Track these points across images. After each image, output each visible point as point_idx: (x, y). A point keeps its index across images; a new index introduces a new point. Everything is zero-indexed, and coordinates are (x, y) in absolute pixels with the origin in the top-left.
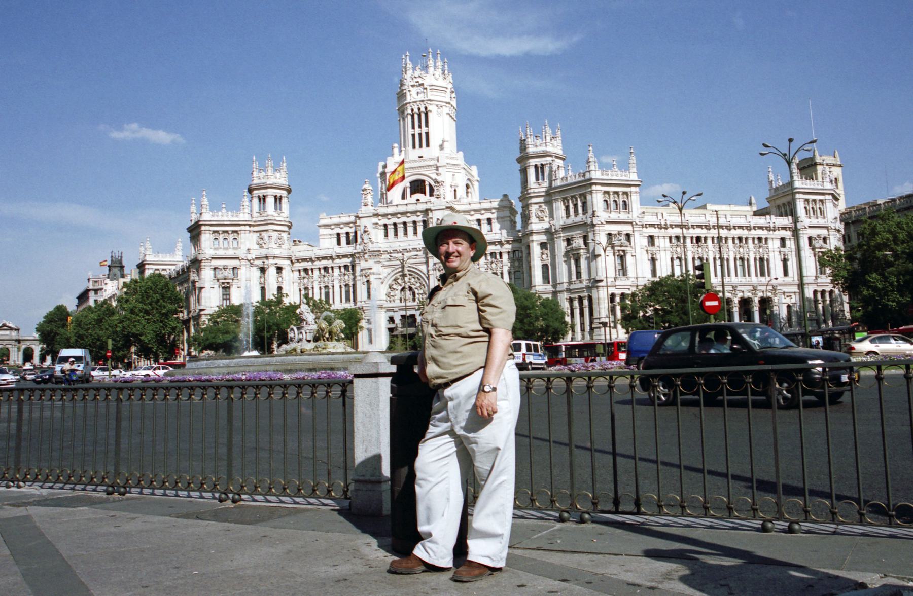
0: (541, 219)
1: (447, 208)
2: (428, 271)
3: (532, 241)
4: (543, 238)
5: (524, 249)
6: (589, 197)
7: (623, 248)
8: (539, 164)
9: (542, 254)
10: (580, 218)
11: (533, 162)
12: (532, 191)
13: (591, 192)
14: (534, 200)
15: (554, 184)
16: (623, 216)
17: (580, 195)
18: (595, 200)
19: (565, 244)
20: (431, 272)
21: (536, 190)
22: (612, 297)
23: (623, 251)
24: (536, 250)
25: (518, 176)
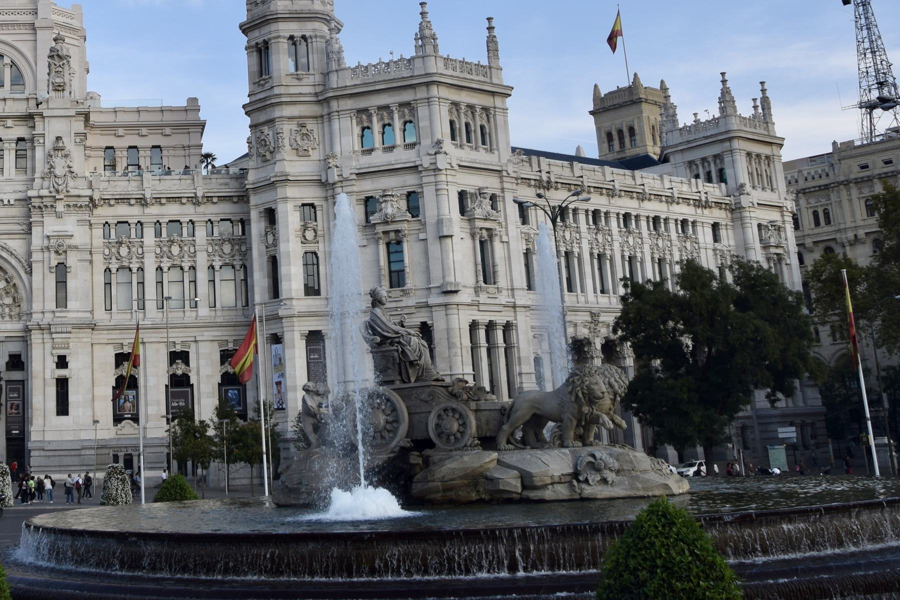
0: (301, 153)
1: (78, 114)
2: (30, 254)
3: (285, 199)
4: (311, 194)
5: (254, 215)
6: (422, 111)
7: (488, 225)
8: (298, 34)
9: (305, 228)
10: (401, 157)
11: (287, 28)
12: (282, 90)
13: (428, 100)
14: (287, 111)
15: (334, 81)
16: (482, 157)
17: (402, 105)
18: (436, 117)
19: (361, 209)
20: (36, 256)
21: (293, 90)
22: (473, 326)
23: (488, 230)
24: (290, 220)
25: (240, 62)
